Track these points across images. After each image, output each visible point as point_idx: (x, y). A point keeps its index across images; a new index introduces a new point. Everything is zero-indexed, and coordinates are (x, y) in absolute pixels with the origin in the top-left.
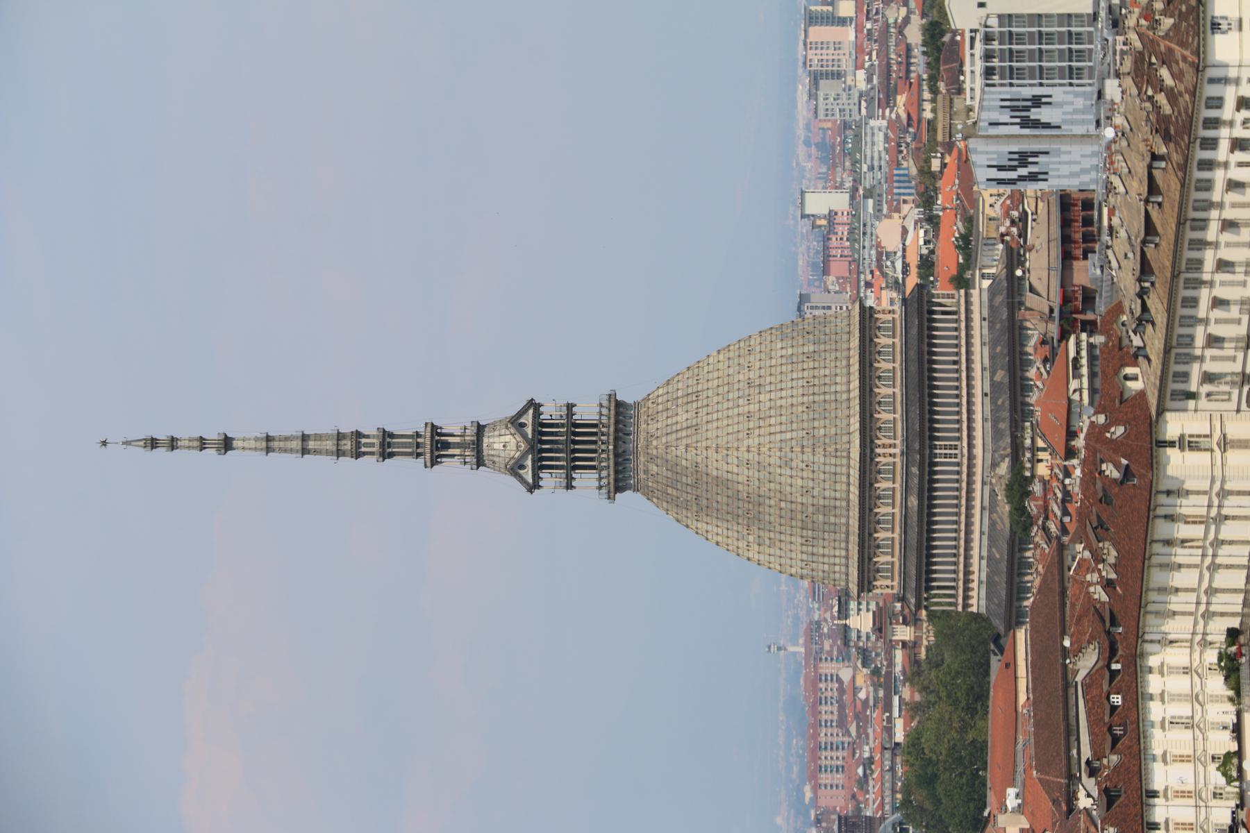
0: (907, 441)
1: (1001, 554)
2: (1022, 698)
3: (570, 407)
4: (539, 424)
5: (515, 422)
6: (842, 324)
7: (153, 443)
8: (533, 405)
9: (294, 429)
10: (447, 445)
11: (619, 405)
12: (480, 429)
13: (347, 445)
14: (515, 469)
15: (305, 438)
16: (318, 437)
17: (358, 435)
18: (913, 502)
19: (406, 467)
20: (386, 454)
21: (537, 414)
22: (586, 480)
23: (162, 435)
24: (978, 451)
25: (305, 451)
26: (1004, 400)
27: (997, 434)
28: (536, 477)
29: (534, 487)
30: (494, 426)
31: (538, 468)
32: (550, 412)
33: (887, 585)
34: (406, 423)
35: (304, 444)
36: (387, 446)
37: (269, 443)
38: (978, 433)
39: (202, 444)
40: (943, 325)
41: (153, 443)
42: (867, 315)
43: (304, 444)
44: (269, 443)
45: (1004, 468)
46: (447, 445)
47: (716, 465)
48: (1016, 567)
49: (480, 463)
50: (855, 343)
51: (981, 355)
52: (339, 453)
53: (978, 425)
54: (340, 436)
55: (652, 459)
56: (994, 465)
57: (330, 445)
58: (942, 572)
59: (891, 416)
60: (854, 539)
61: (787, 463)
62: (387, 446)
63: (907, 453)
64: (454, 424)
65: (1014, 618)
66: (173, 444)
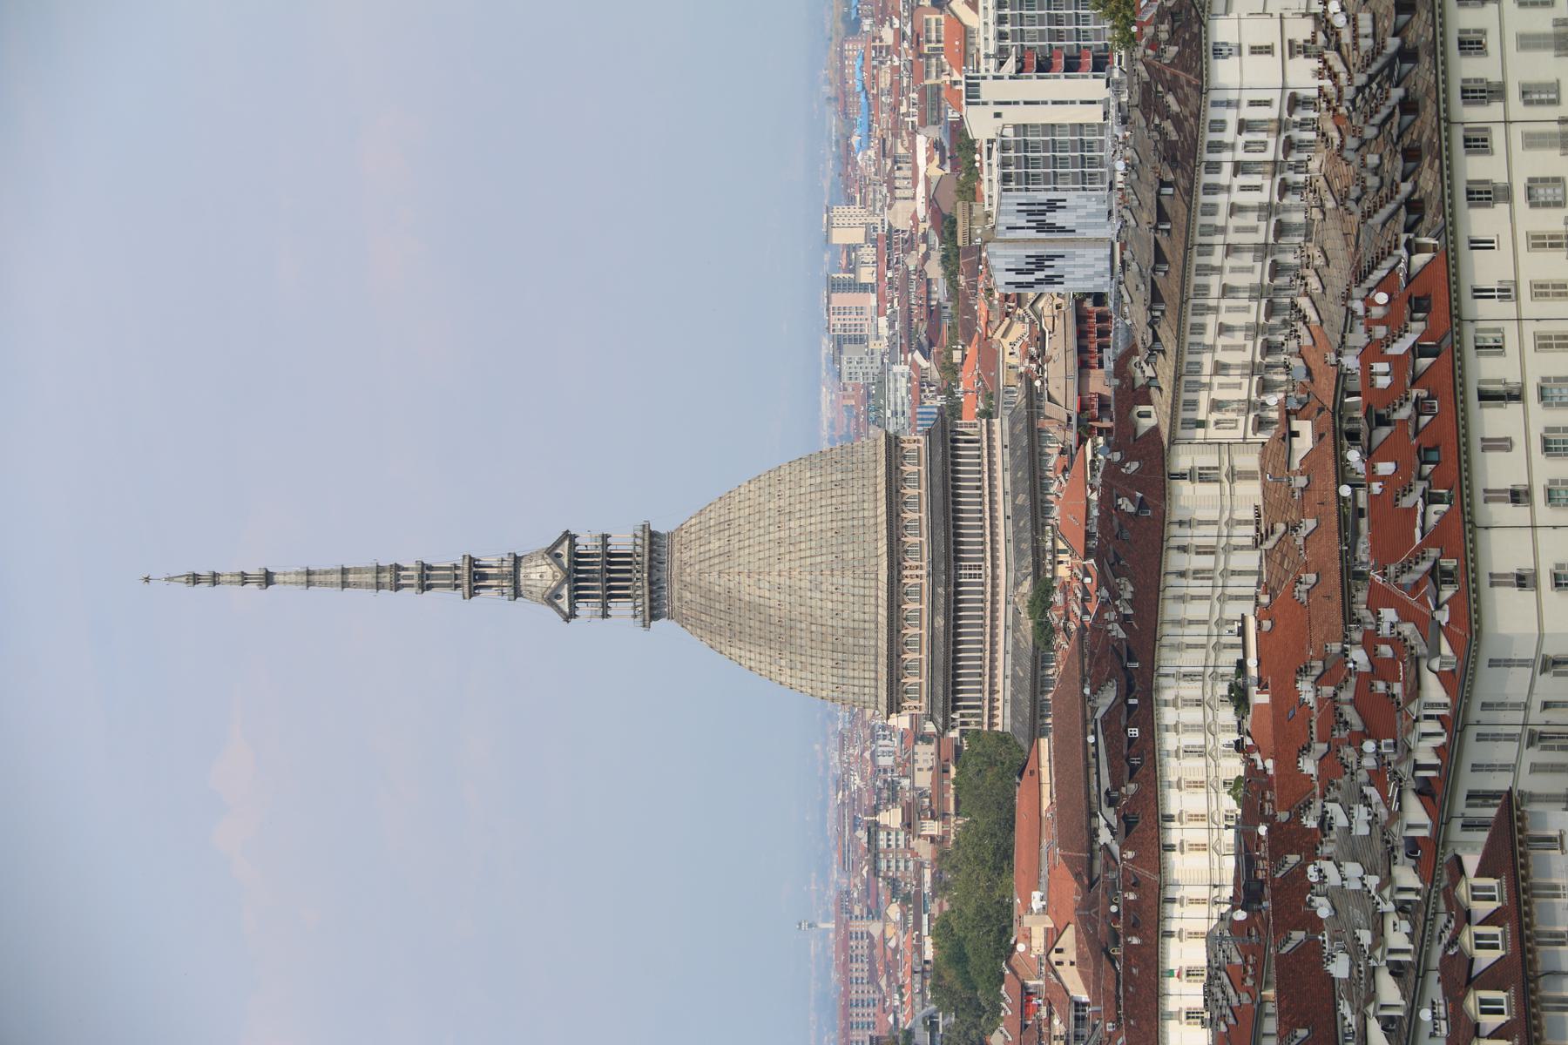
0: (933, 562)
1: (1025, 672)
2: (1046, 802)
3: (605, 537)
4: (575, 556)
5: (552, 553)
6: (868, 454)
7: (195, 579)
8: (569, 537)
9: (335, 563)
10: (484, 577)
11: (652, 535)
12: (517, 560)
13: (386, 578)
14: (552, 598)
15: (344, 571)
16: (358, 571)
17: (398, 568)
18: (940, 622)
19: (444, 600)
20: (425, 587)
21: (573, 545)
22: (620, 608)
23: (204, 571)
24: (1002, 571)
25: (345, 584)
26: (1025, 522)
27: (1019, 554)
28: (572, 606)
29: (570, 616)
30: (531, 557)
31: (575, 597)
32: (587, 543)
33: (917, 704)
34: (445, 555)
35: (345, 577)
36: (426, 578)
37: (309, 577)
38: (1001, 554)
39: (244, 579)
40: (966, 453)
41: (195, 579)
42: (893, 443)
43: (345, 577)
44: (309, 577)
45: (1026, 587)
46: (484, 577)
47: (749, 590)
48: (1038, 683)
49: (517, 593)
50: (882, 470)
51: (1003, 480)
52: (379, 586)
53: (1001, 546)
54: (379, 570)
55: (685, 586)
56: (1017, 584)
57: (369, 578)
58: (968, 693)
59: (918, 540)
60: (883, 660)
61: (817, 587)
62: (426, 578)
63: (933, 574)
64: (491, 556)
65: (1036, 732)
66: (215, 579)
